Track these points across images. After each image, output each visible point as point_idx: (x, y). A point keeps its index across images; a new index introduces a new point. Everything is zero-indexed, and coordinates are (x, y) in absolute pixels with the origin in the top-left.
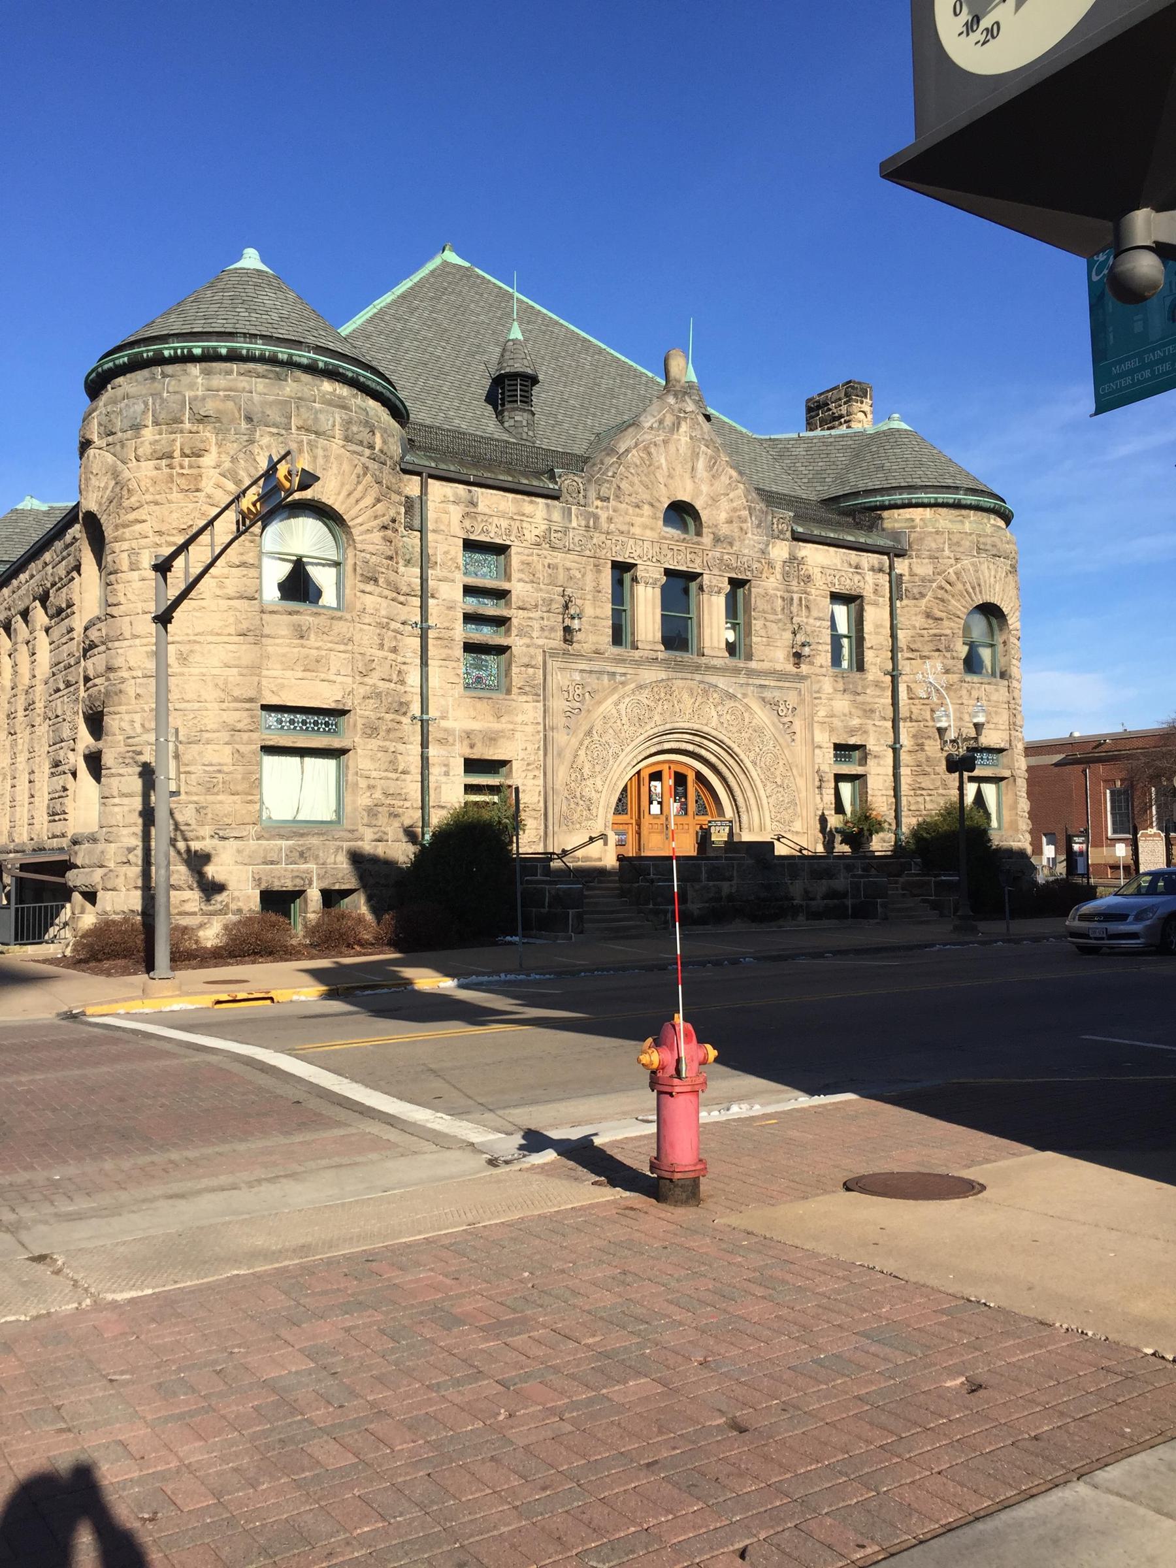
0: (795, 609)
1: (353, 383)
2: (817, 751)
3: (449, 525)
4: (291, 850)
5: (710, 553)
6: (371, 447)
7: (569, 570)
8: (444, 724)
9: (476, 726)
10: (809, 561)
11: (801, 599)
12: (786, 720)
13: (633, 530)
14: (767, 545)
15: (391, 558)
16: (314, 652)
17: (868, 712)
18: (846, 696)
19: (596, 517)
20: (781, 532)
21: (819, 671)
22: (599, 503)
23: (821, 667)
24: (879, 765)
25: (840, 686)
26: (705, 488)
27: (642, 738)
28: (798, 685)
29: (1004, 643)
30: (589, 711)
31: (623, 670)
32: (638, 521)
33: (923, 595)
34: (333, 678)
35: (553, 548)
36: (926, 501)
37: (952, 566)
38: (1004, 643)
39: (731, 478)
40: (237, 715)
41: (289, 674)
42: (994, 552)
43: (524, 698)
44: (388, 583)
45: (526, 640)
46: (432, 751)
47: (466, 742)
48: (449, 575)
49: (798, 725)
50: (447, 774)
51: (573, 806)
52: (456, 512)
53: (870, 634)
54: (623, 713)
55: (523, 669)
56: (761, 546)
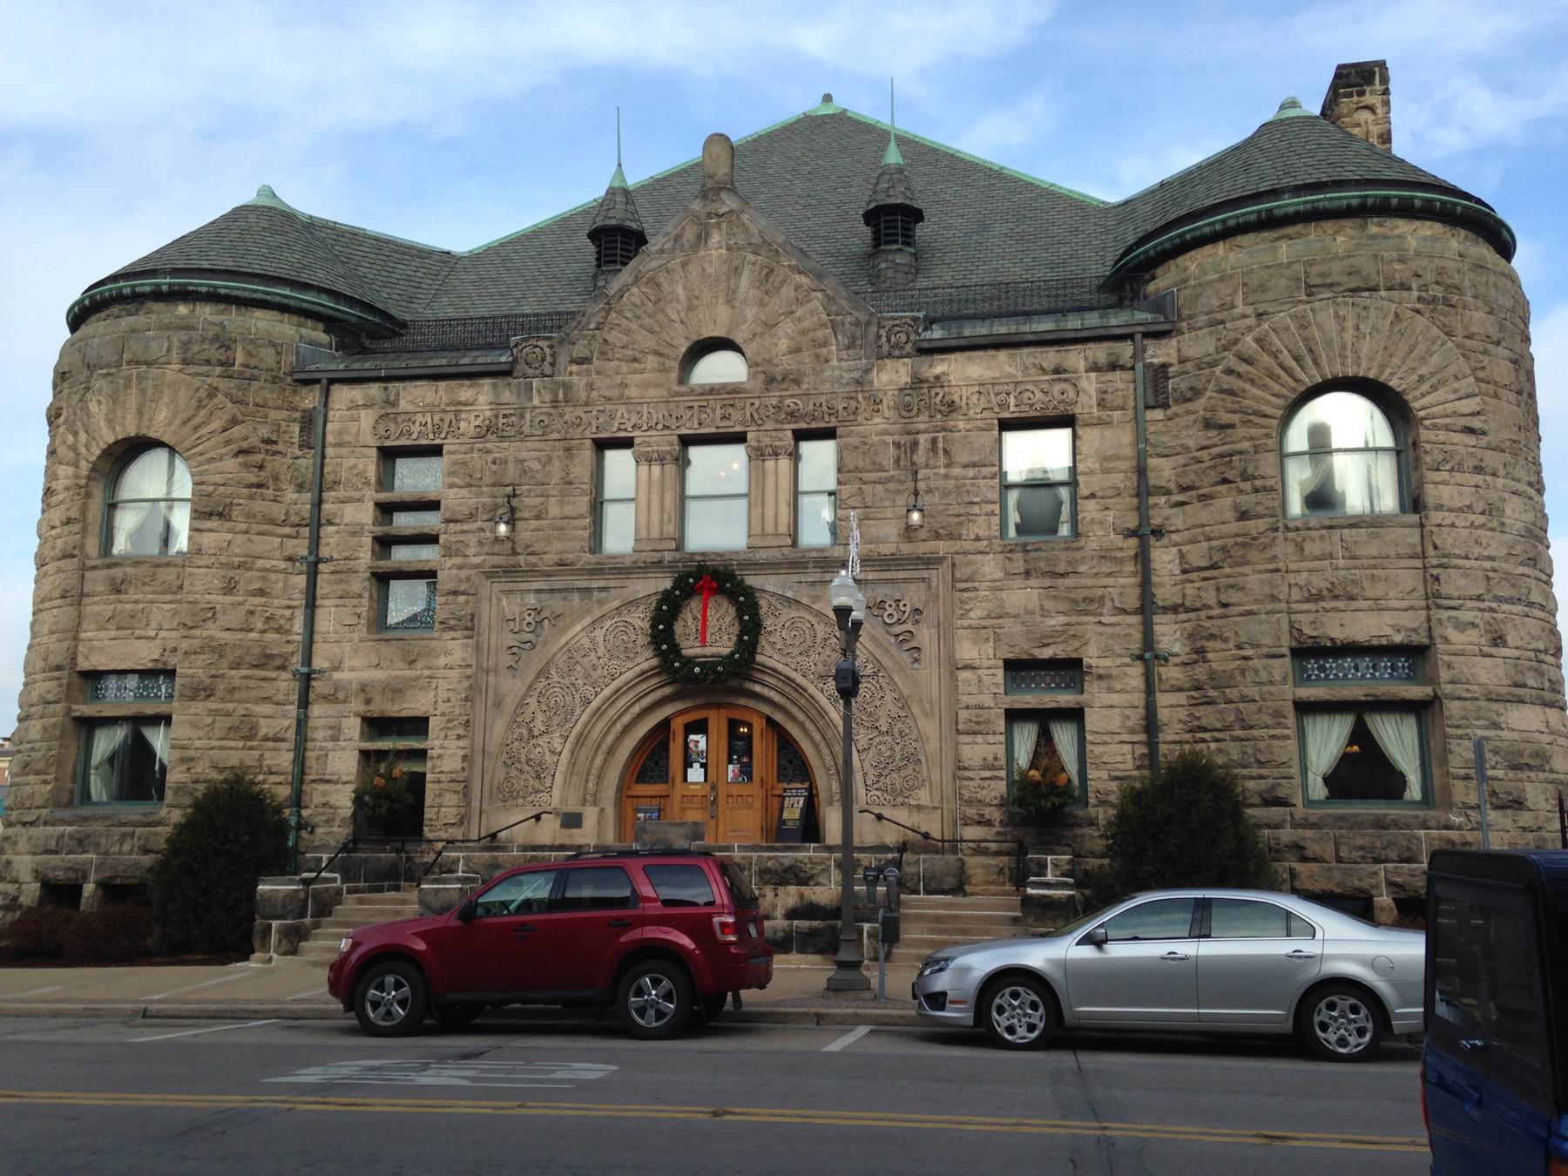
0: (921, 456)
1: (213, 297)
2: (963, 675)
3: (358, 434)
4: (71, 836)
5: (757, 403)
6: (227, 364)
7: (521, 461)
8: (336, 675)
9: (378, 675)
10: (953, 378)
11: (934, 441)
12: (898, 629)
13: (627, 392)
14: (868, 371)
15: (260, 486)
16: (129, 606)
17: (1086, 605)
18: (1032, 582)
19: (567, 387)
20: (898, 346)
21: (967, 546)
22: (575, 368)
23: (978, 539)
24: (1111, 690)
25: (1019, 565)
26: (750, 313)
27: (630, 675)
28: (925, 574)
29: (1415, 444)
30: (546, 643)
31: (602, 584)
32: (636, 378)
33: (1196, 393)
34: (153, 633)
35: (502, 438)
36: (1207, 230)
37: (1250, 329)
38: (1415, 444)
39: (797, 288)
40: (49, 684)
41: (103, 634)
42: (1353, 285)
43: (452, 634)
44: (250, 516)
45: (457, 560)
46: (316, 710)
47: (362, 697)
48: (356, 495)
49: (925, 636)
50: (335, 738)
51: (514, 773)
52: (367, 418)
53: (1091, 473)
54: (600, 640)
55: (451, 597)
56: (855, 375)
